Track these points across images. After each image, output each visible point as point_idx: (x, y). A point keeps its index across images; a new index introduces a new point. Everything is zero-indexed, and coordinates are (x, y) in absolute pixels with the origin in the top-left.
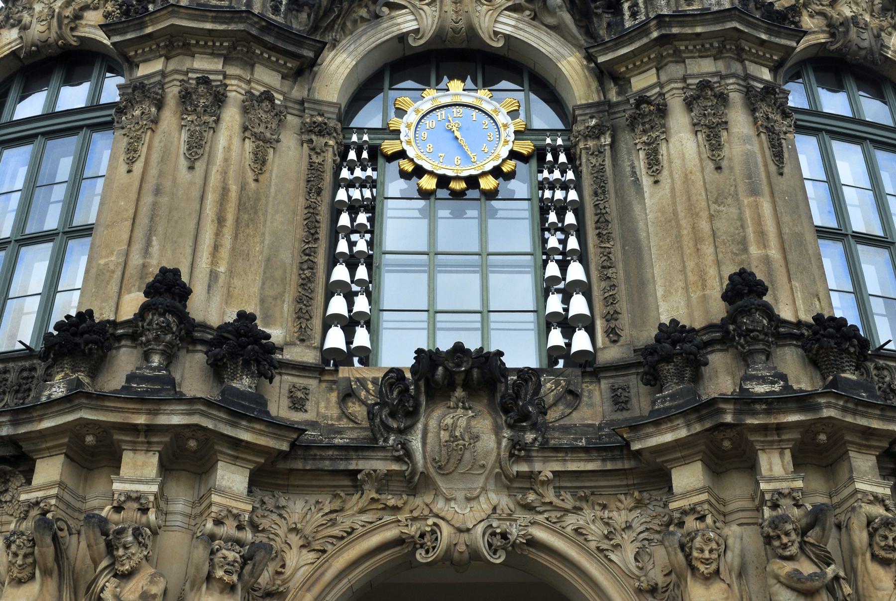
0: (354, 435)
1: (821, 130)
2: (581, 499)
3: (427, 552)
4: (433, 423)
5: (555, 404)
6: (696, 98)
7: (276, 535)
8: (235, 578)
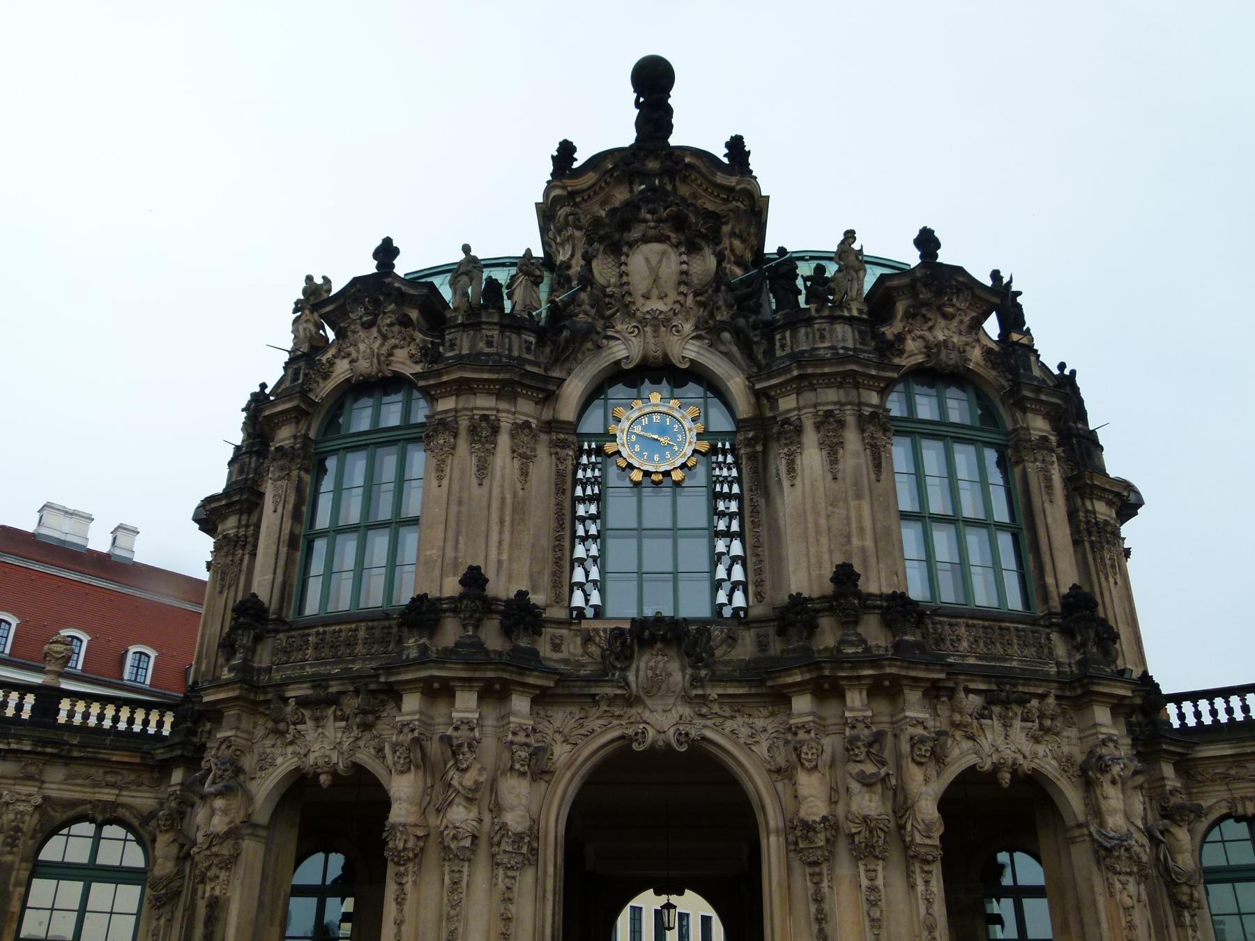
0: (591, 668)
1: (913, 432)
2: (735, 711)
3: (639, 744)
4: (642, 665)
5: (721, 645)
6: (822, 423)
7: (547, 734)
8: (526, 768)
